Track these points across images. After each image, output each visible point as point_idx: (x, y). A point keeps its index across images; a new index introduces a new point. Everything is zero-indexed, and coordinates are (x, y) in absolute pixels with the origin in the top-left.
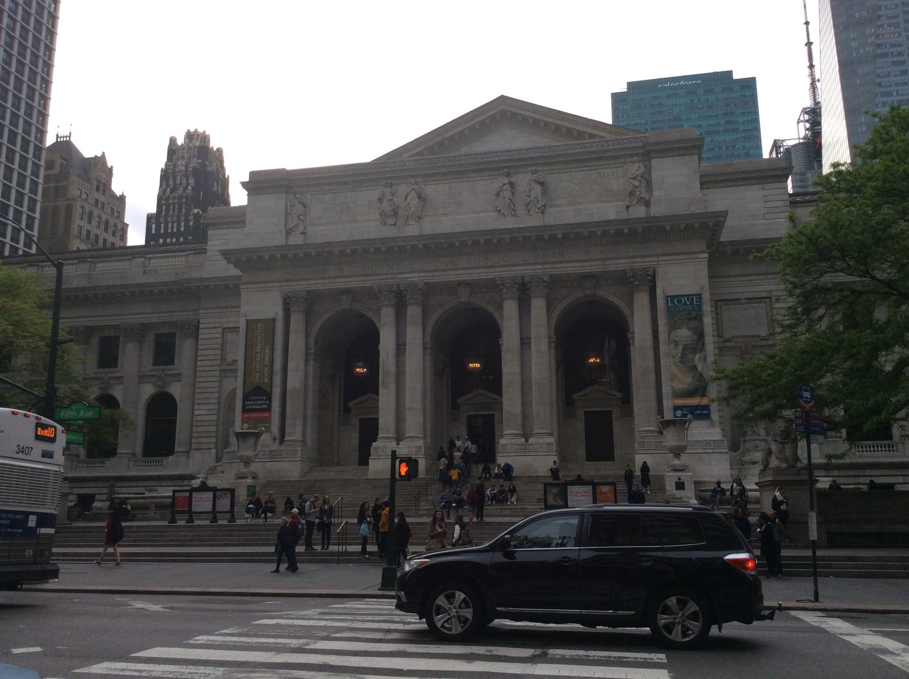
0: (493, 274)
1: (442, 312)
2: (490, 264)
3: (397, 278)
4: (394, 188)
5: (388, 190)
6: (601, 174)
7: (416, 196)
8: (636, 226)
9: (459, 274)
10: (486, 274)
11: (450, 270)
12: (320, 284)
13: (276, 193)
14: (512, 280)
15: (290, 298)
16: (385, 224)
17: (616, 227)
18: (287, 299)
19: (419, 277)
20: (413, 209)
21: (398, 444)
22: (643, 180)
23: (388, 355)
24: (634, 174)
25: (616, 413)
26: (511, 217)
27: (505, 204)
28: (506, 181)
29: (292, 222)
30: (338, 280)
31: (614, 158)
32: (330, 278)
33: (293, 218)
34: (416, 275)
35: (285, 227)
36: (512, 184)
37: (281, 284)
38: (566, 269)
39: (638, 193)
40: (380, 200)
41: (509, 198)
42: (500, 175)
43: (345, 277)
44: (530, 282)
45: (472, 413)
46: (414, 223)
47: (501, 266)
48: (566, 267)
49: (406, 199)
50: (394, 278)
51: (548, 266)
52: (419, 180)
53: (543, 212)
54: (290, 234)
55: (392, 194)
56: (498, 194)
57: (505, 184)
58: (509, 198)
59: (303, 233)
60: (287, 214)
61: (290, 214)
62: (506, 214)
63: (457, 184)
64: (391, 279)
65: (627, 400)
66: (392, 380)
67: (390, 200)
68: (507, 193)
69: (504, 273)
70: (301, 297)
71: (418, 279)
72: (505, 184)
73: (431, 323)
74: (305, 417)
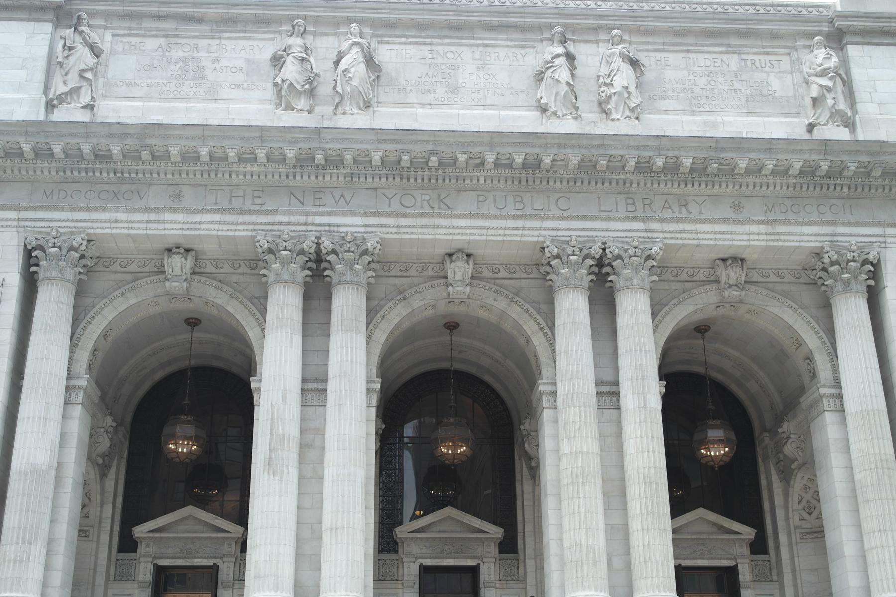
1: (404, 314)
2: (528, 212)
3: (313, 224)
5: (296, 42)
6: (749, 63)
7: (362, 59)
8: (844, 158)
10: (520, 232)
11: (439, 216)
12: (122, 222)
13: (29, 20)
14: (581, 250)
15: (41, 248)
16: (290, 108)
17: (806, 157)
18: (34, 249)
19: (366, 226)
20: (355, 82)
22: (838, 79)
23: (284, 398)
24: (821, 65)
25: (745, 574)
26: (572, 121)
27: (557, 93)
28: (560, 50)
29: (65, 83)
30: (168, 217)
31: (774, 36)
32: (147, 210)
33: (66, 74)
34: (358, 220)
36: (570, 57)
37: (24, 215)
38: (694, 236)
39: (830, 102)
40: (277, 61)
41: (568, 83)
42: (541, 40)
43: (185, 211)
44: (619, 257)
45: (428, 562)
46: (356, 111)
47: (554, 218)
48: (696, 233)
49: (337, 63)
50: (306, 224)
51: (655, 226)
52: (367, 31)
53: (637, 118)
54: (54, 107)
55: (306, 49)
56: (539, 77)
57: (558, 56)
58: (568, 83)
59: (90, 107)
60: (52, 65)
61: (61, 64)
62: (560, 114)
63: (450, 48)
64: (299, 224)
65: (759, 546)
66: (290, 456)
67: (302, 60)
68: (564, 74)
69: (560, 233)
70: (72, 249)
71: (362, 230)
72: (558, 56)
73: (381, 337)
74: (50, 542)
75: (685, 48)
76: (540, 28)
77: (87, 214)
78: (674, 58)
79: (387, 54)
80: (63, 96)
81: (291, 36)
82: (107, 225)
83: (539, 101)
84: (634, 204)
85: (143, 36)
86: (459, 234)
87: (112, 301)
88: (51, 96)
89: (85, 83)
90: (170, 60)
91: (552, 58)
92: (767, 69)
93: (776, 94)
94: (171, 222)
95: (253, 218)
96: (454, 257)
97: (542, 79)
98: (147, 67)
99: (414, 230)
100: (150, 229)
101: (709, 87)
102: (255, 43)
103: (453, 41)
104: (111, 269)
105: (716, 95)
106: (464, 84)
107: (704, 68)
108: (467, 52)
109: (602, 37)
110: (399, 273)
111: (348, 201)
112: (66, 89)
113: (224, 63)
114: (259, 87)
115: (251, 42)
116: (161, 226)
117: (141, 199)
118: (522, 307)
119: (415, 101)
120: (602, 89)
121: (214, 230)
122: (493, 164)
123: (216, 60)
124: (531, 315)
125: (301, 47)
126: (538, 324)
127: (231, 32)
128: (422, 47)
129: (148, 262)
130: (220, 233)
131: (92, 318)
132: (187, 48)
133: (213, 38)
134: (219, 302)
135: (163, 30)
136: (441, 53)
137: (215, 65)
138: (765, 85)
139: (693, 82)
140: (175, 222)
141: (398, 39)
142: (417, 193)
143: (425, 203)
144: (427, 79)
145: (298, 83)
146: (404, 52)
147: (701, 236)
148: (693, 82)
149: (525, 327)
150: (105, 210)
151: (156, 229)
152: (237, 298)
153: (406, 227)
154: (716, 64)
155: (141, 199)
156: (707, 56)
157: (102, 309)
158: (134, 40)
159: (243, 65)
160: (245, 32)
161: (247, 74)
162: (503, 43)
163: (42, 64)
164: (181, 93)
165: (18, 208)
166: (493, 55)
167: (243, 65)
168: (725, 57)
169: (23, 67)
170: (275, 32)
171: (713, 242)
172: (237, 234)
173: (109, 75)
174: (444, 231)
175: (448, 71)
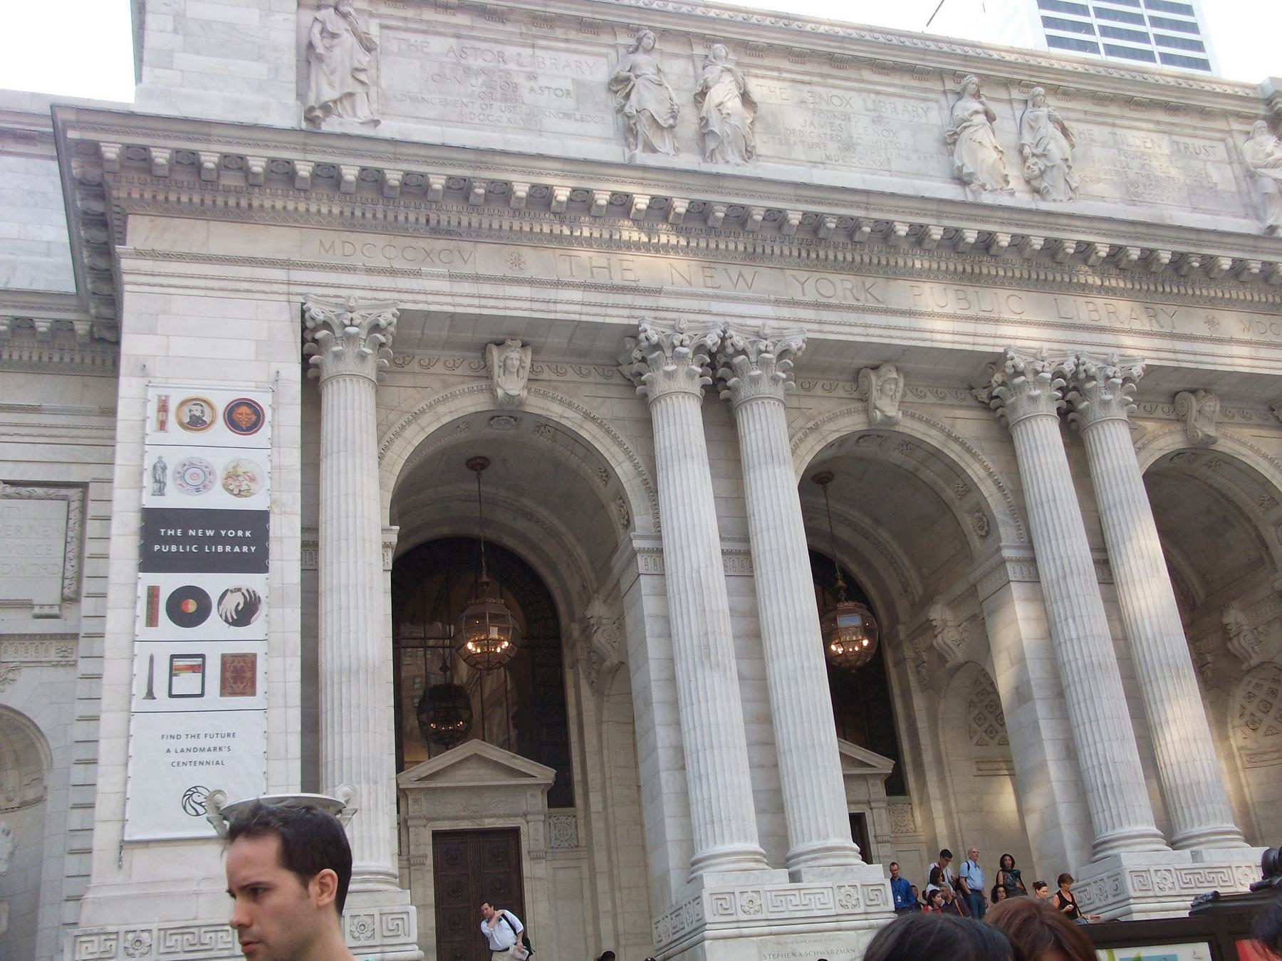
0: (991, 341)
1: (818, 448)
6: (1182, 147)
7: (737, 93)
9: (895, 328)
15: (326, 325)
20: (733, 121)
21: (794, 877)
24: (1269, 155)
28: (978, 106)
29: (331, 85)
34: (768, 310)
35: (301, 96)
37: (297, 275)
40: (621, 84)
46: (740, 161)
57: (977, 112)
62: (988, 187)
72: (977, 112)
75: (1110, 120)
76: (940, 74)
77: (390, 279)
78: (1099, 132)
79: (760, 88)
80: (331, 104)
81: (636, 49)
82: (422, 297)
83: (960, 169)
85: (424, 32)
86: (897, 338)
87: (416, 416)
88: (312, 102)
89: (359, 89)
91: (971, 115)
92: (1202, 156)
93: (1219, 188)
94: (515, 299)
95: (628, 299)
96: (883, 370)
97: (954, 142)
98: (436, 77)
99: (840, 329)
100: (485, 307)
102: (583, 58)
103: (838, 82)
104: (406, 368)
106: (859, 141)
108: (858, 103)
109: (1016, 94)
110: (803, 392)
111: (750, 282)
112: (335, 95)
113: (543, 81)
114: (596, 119)
115: (577, 57)
116: (501, 303)
117: (466, 262)
118: (963, 444)
119: (803, 157)
120: (1031, 161)
121: (575, 313)
122: (936, 244)
123: (531, 76)
124: (974, 456)
126: (986, 468)
127: (546, 38)
128: (800, 86)
129: (459, 362)
130: (584, 318)
132: (489, 57)
133: (524, 45)
134: (568, 424)
135: (455, 26)
136: (825, 96)
137: (532, 83)
138: (1204, 175)
139: (1125, 164)
140: (521, 299)
141: (769, 73)
142: (836, 278)
143: (848, 294)
145: (659, 116)
146: (778, 92)
147: (1180, 356)
148: (1125, 164)
149: (969, 471)
150: (417, 274)
151: (492, 307)
152: (594, 419)
153: (830, 323)
155: (466, 262)
156: (1134, 132)
157: (403, 428)
158: (413, 37)
159: (568, 85)
160: (567, 41)
161: (577, 100)
162: (898, 91)
163: (289, 59)
164: (490, 118)
165: (286, 264)
167: (570, 87)
169: (260, 58)
170: (609, 46)
171: (1193, 366)
172: (608, 320)
173: (383, 83)
174: (878, 332)
175: (837, 122)
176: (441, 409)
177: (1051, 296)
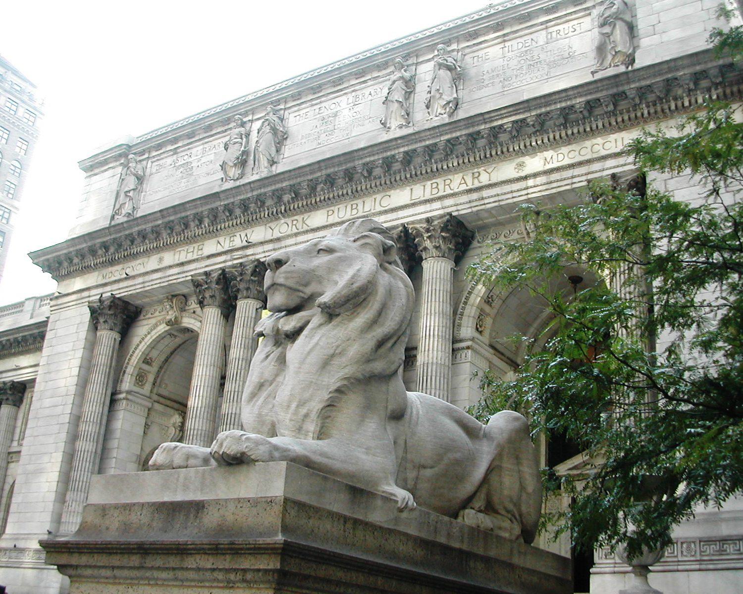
4: (249, 125)
57: (394, 82)
63: (334, 101)
72: (394, 82)
84: (437, 187)
90: (178, 168)
101: (520, 66)
104: (147, 317)
105: (524, 72)
107: (516, 52)
125: (237, 135)
131: (134, 352)
137: (199, 164)
144: (317, 130)
147: (486, 201)
154: (527, 45)
156: (519, 40)
159: (212, 157)
166: (360, 97)
168: (533, 36)
176: (154, 332)
177: (408, 188)
